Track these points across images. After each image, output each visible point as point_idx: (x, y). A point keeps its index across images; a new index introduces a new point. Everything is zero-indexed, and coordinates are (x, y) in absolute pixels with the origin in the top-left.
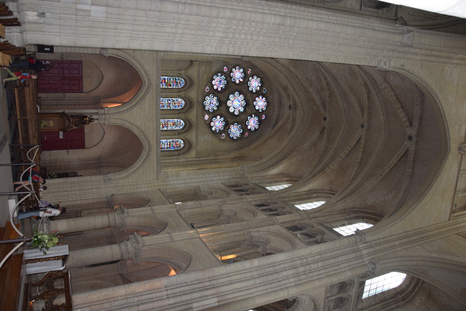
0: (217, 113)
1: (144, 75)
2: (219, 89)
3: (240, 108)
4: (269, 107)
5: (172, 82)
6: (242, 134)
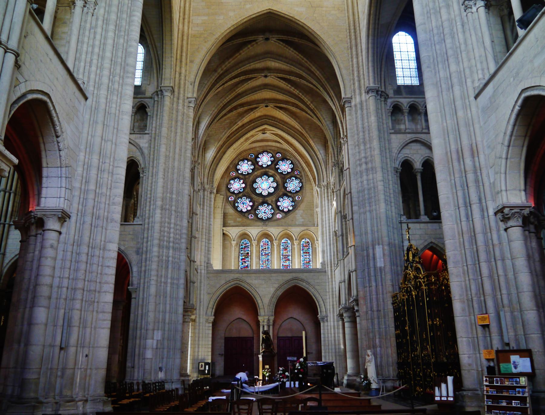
0: (274, 206)
1: (230, 284)
2: (251, 204)
3: (269, 181)
4: (269, 150)
5: (245, 251)
6: (296, 178)
